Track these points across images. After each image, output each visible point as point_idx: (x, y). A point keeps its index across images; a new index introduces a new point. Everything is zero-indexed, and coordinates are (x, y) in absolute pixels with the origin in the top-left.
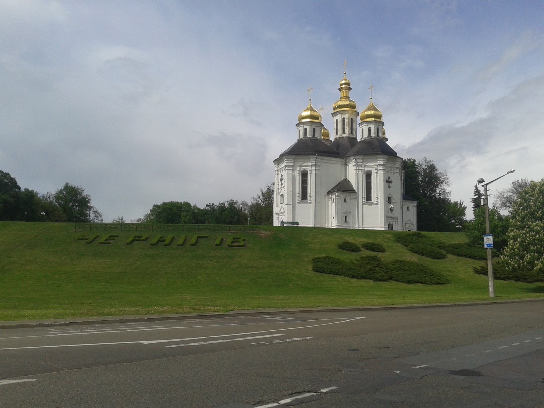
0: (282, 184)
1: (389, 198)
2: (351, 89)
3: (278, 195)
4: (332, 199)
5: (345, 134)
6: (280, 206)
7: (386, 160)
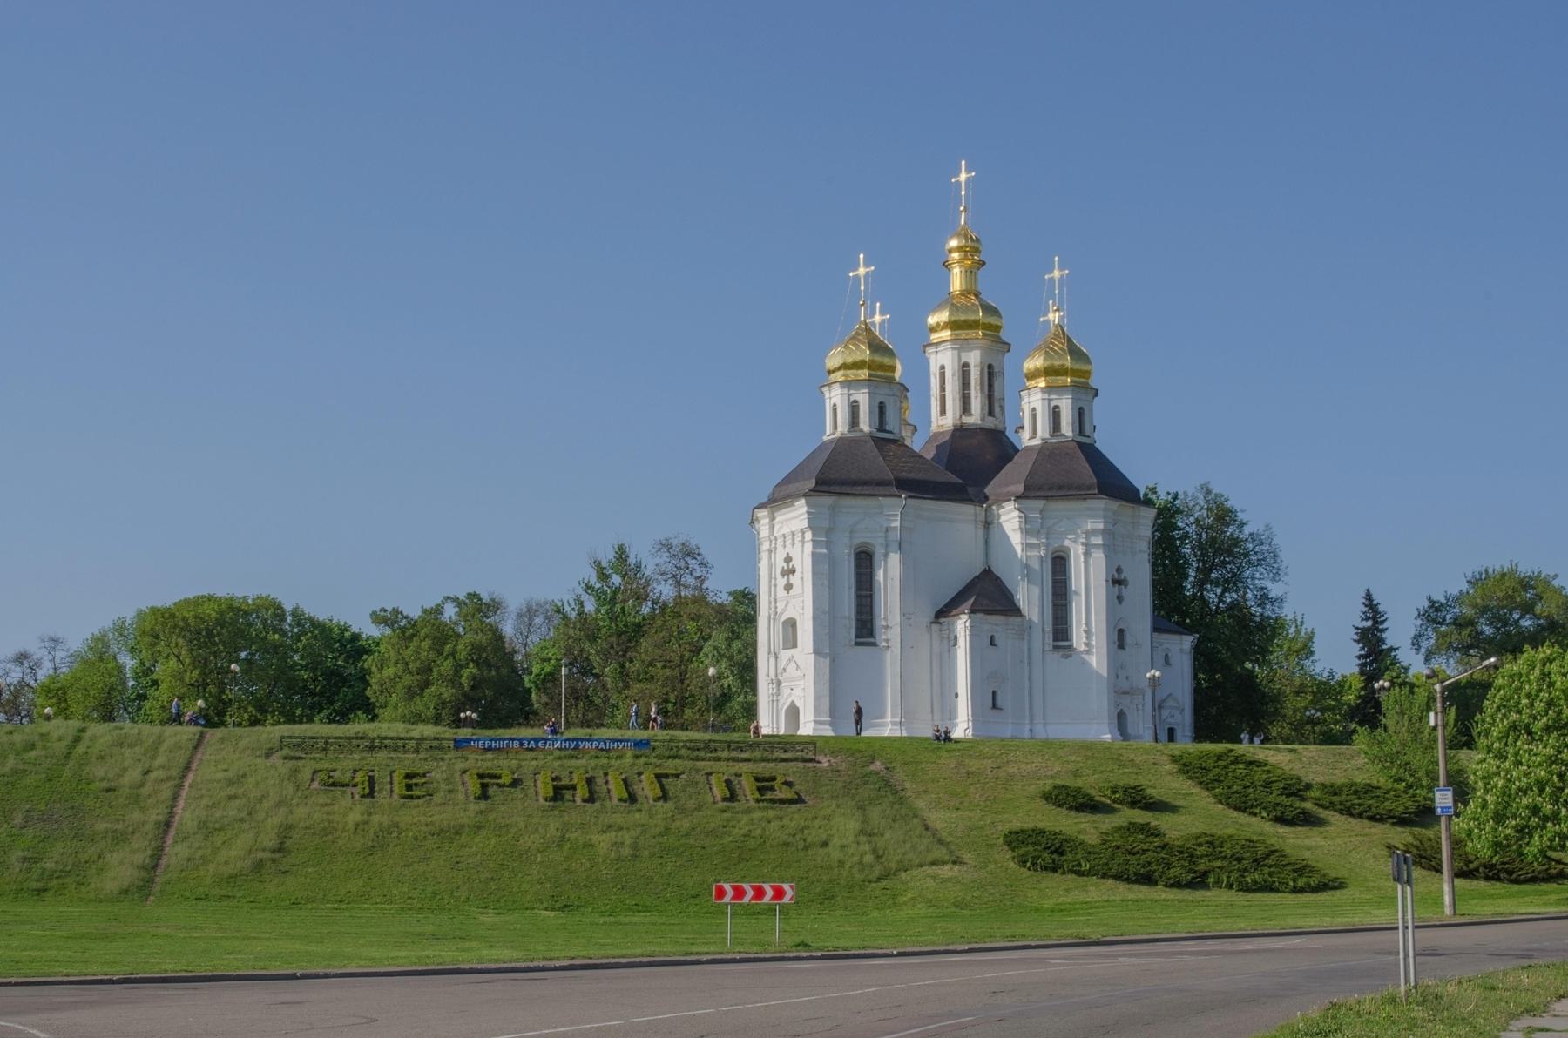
0: (788, 587)
1: (1121, 632)
3: (774, 619)
5: (971, 415)
6: (785, 655)
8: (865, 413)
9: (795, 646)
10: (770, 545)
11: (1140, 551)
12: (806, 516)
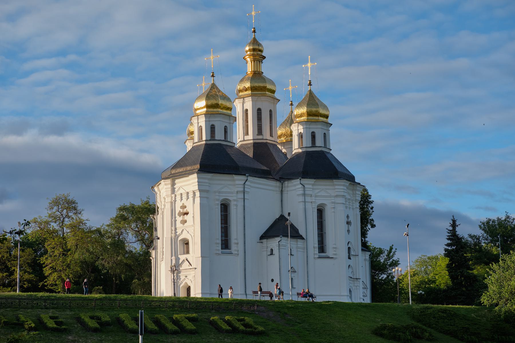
2: (264, 58)
4: (269, 250)
7: (345, 188)
9: (188, 252)
11: (356, 208)
12: (197, 184)
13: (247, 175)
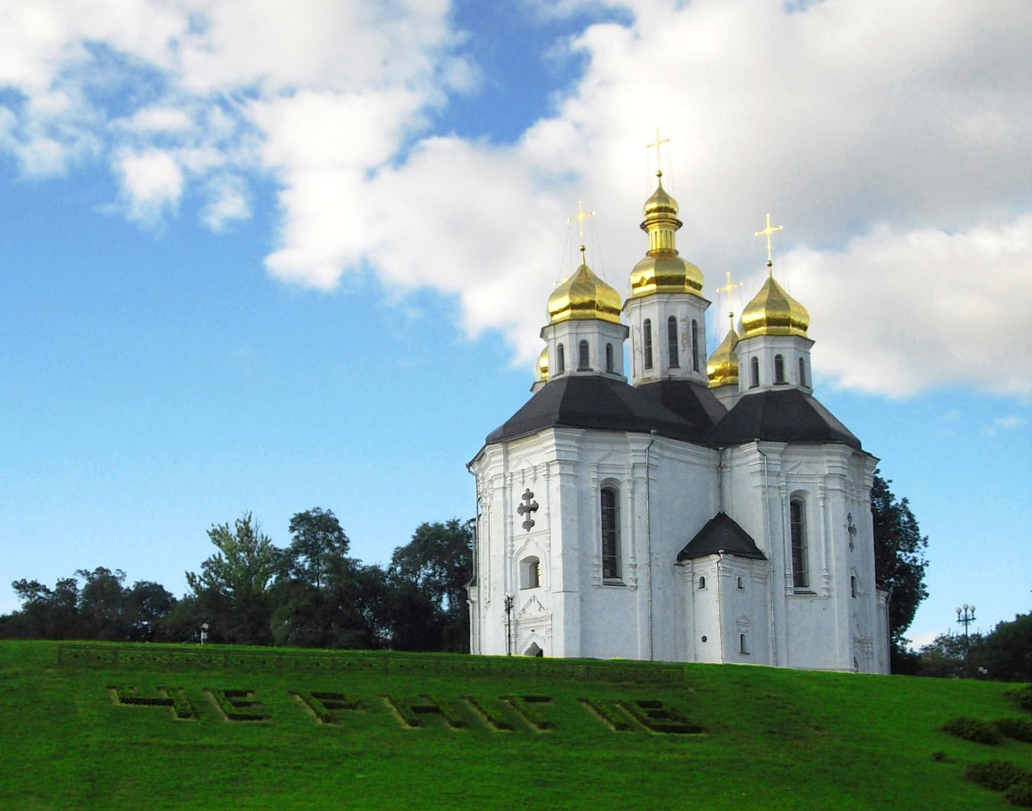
0: (529, 524)
2: (679, 224)
3: (511, 558)
4: (697, 579)
7: (845, 461)
8: (595, 353)
9: (536, 584)
10: (505, 482)
11: (865, 501)
13: (652, 431)
